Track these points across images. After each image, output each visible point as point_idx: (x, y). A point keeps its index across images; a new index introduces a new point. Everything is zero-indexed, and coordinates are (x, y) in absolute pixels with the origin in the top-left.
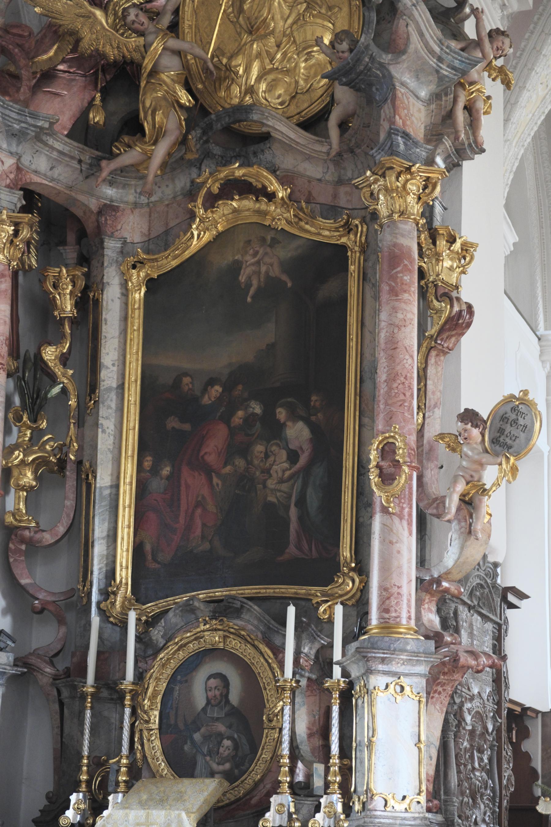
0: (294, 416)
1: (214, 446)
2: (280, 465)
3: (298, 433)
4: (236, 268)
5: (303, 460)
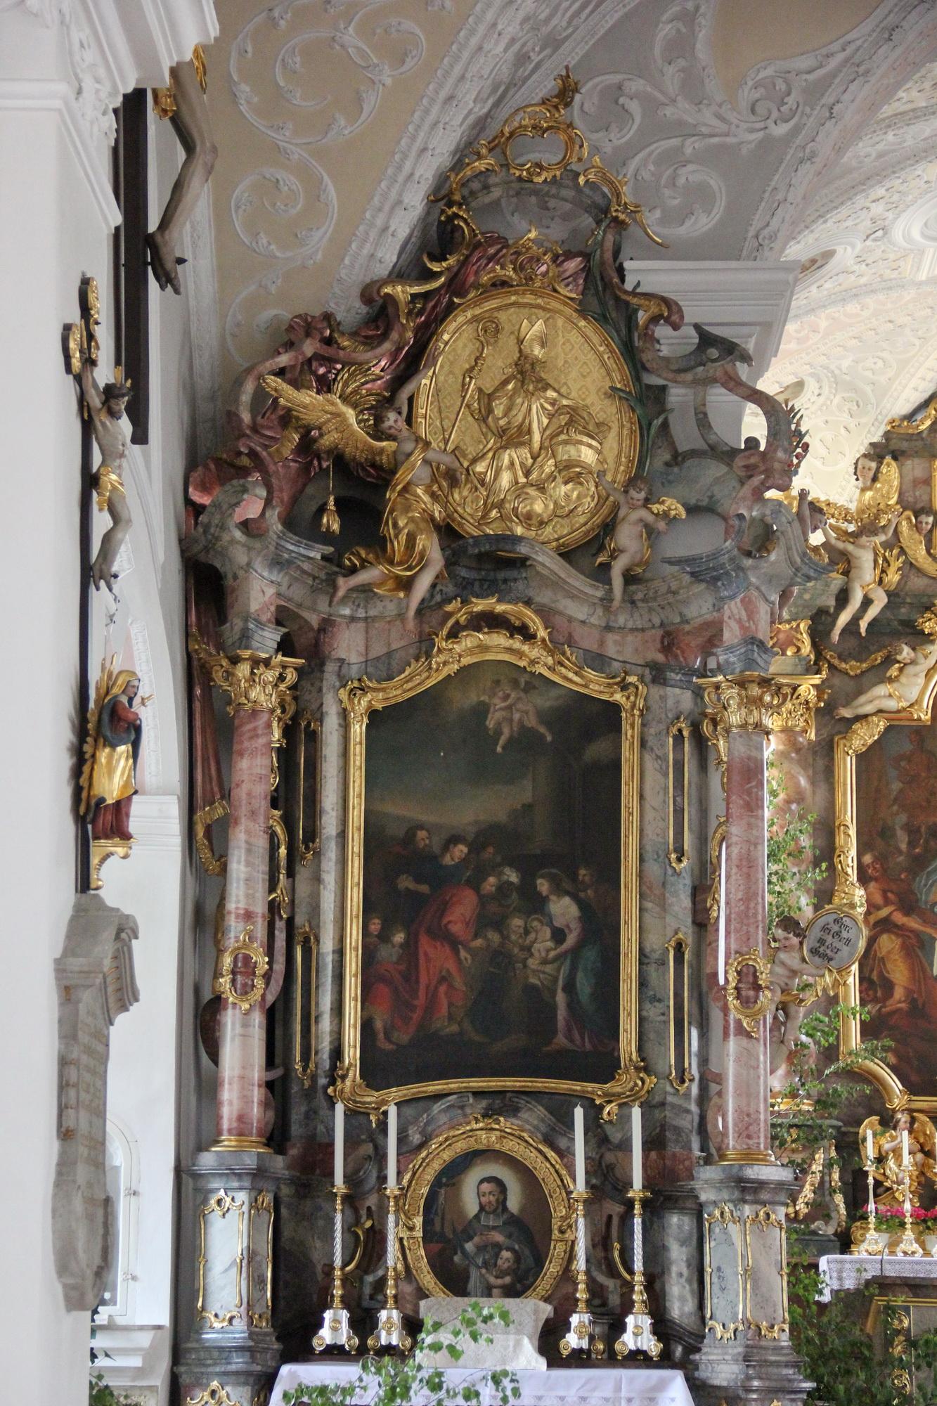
0: (559, 890)
2: (543, 943)
3: (564, 909)
4: (481, 711)
5: (571, 940)
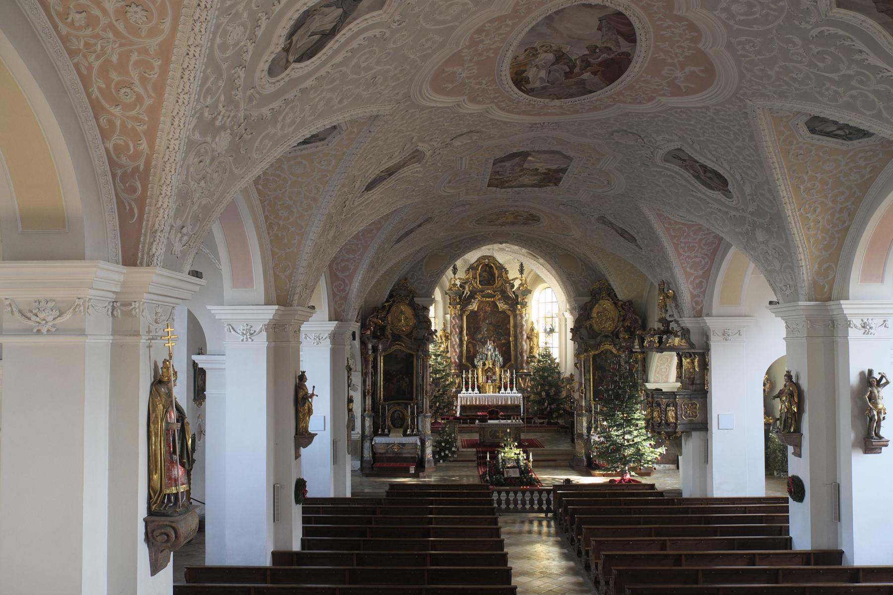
3: (407, 380)
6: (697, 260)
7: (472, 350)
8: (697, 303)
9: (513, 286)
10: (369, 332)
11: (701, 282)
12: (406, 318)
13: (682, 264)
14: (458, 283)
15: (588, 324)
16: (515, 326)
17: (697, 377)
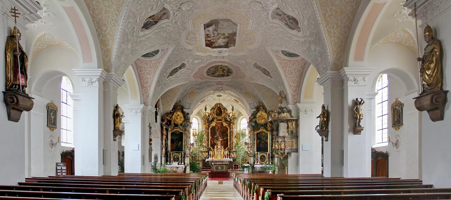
1: (175, 143)
6: (294, 79)
7: (212, 142)
8: (295, 99)
9: (229, 116)
10: (164, 123)
11: (296, 89)
12: (180, 117)
13: (288, 80)
14: (207, 115)
15: (254, 120)
16: (230, 133)
17: (294, 130)
